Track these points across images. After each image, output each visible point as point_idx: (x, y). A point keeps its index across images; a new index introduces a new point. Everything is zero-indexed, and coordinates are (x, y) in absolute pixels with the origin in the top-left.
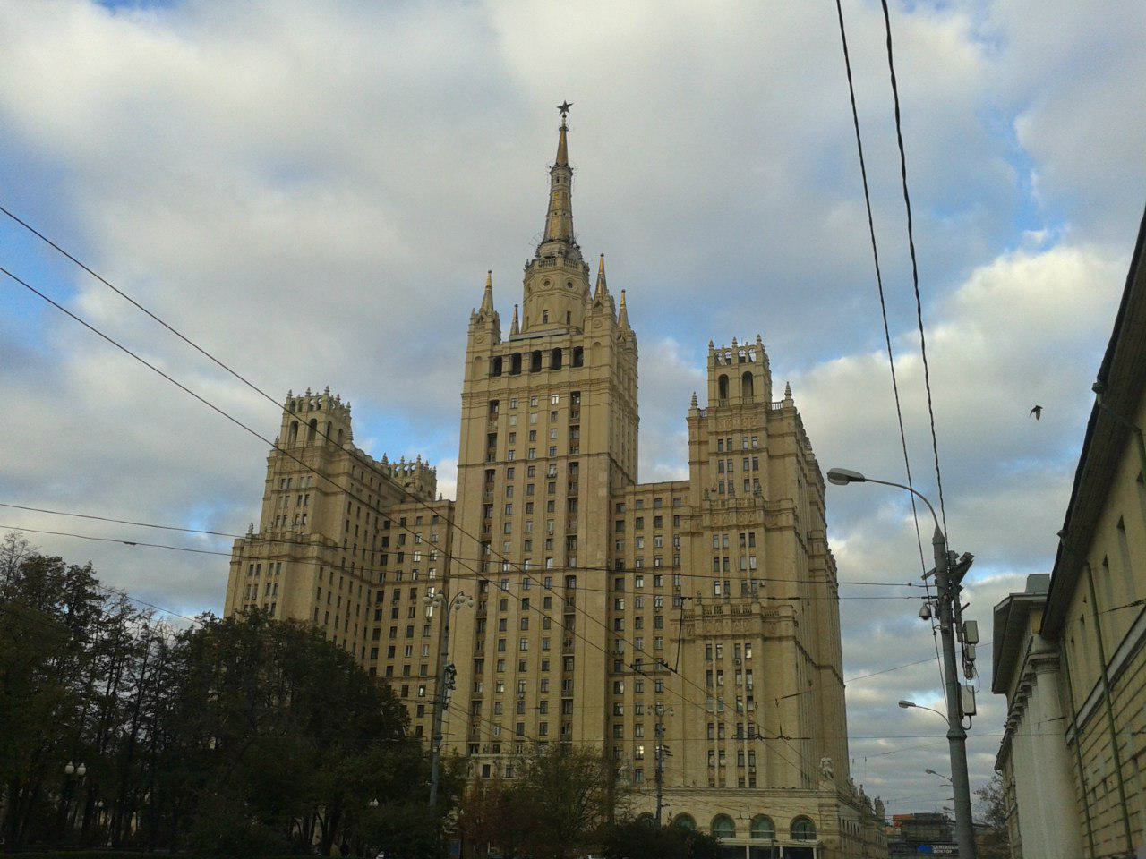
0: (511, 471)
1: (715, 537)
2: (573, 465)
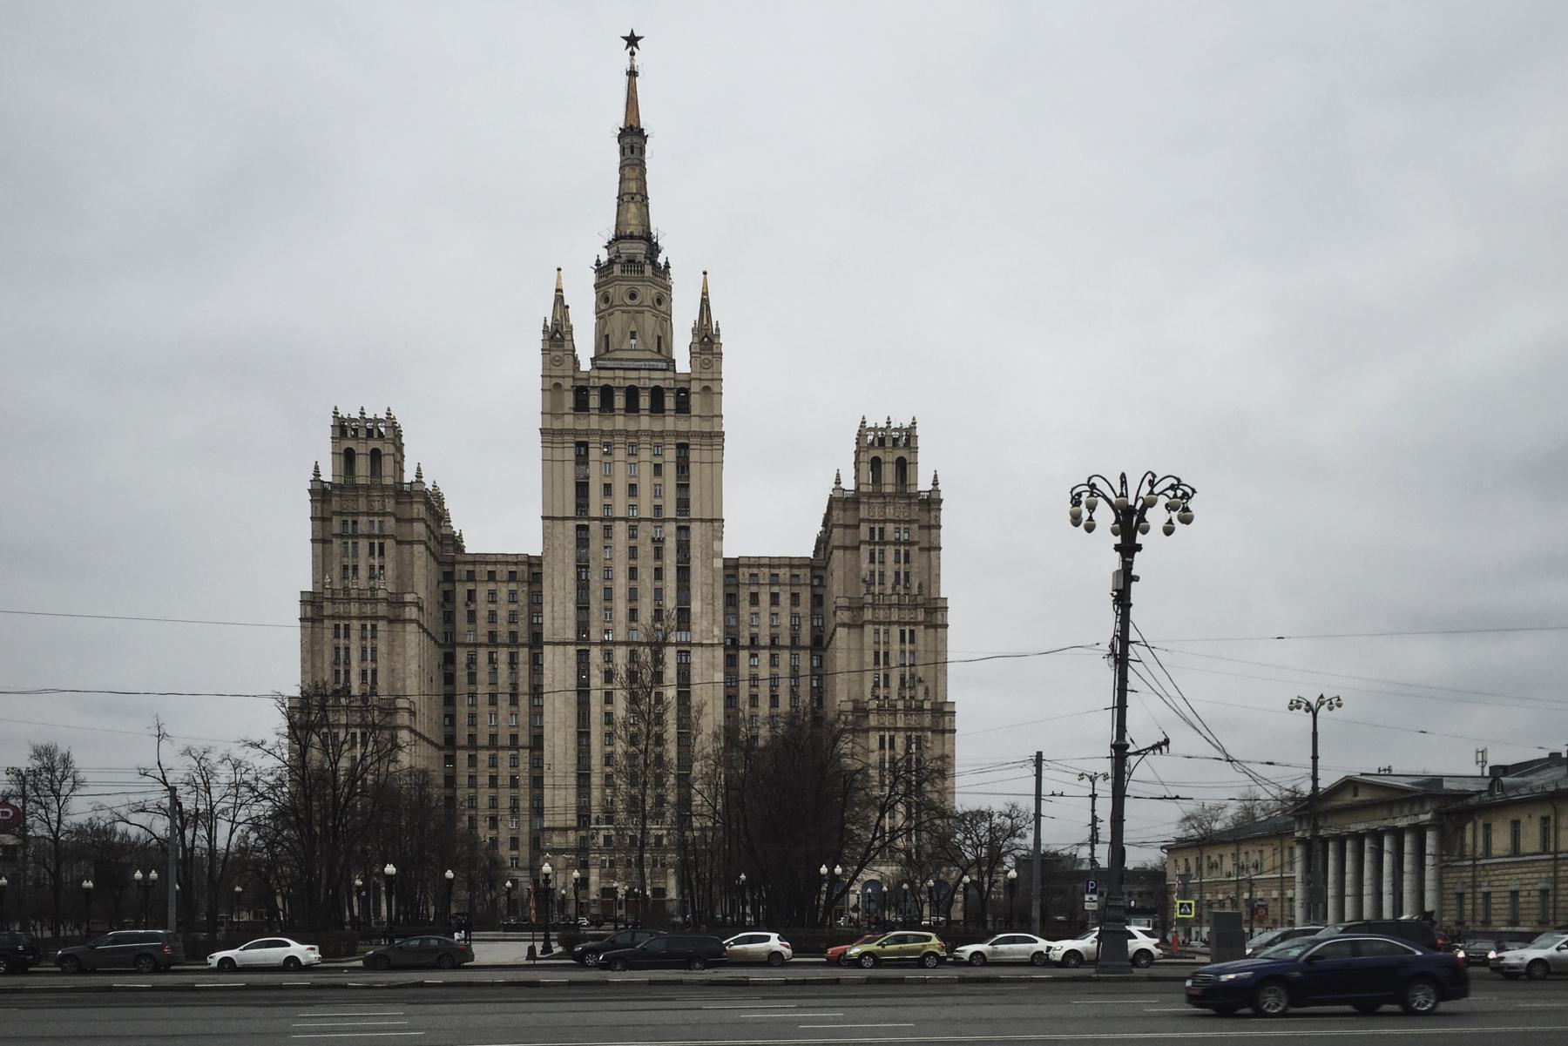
0: (608, 529)
1: (877, 632)
2: (683, 530)
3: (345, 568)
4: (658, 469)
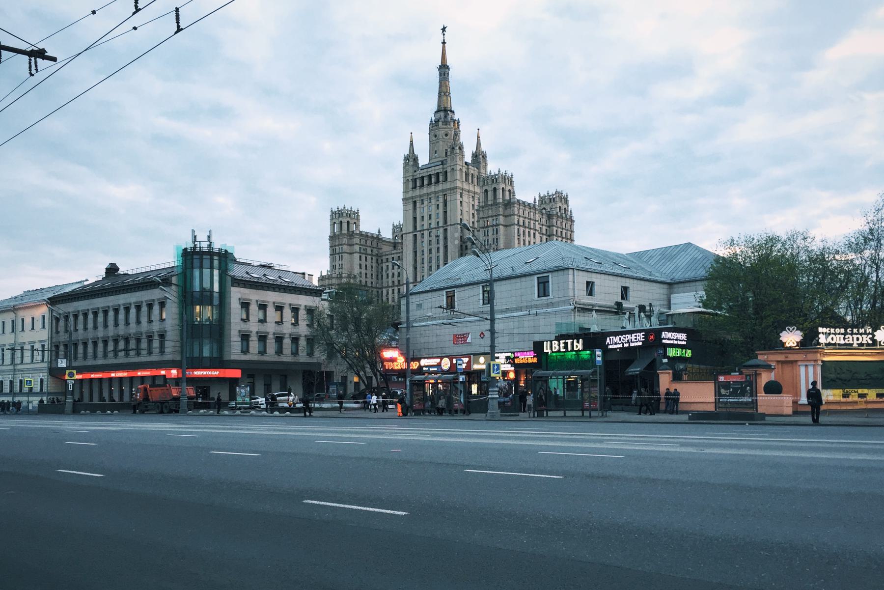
2: (446, 230)
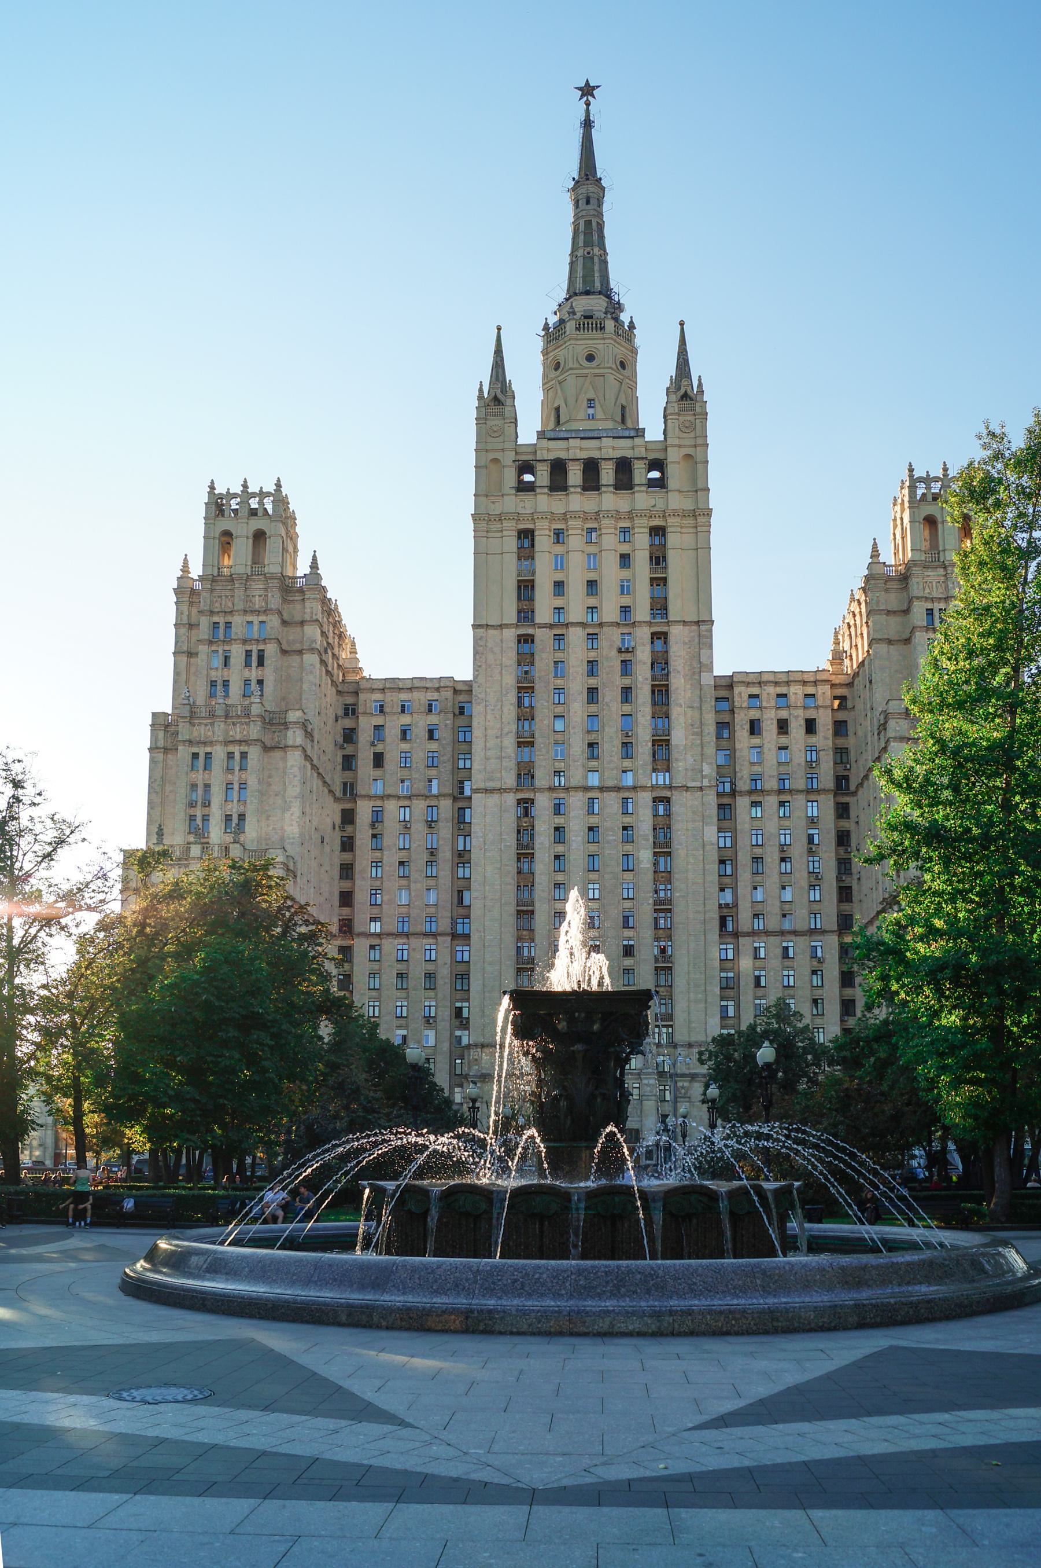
0: (559, 638)
2: (660, 637)
3: (213, 684)
4: (625, 560)
